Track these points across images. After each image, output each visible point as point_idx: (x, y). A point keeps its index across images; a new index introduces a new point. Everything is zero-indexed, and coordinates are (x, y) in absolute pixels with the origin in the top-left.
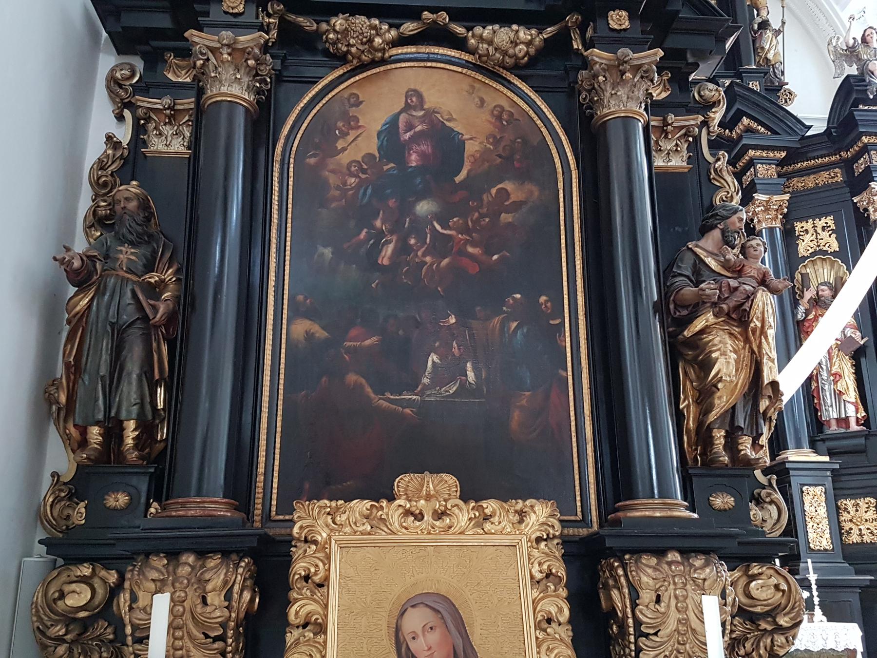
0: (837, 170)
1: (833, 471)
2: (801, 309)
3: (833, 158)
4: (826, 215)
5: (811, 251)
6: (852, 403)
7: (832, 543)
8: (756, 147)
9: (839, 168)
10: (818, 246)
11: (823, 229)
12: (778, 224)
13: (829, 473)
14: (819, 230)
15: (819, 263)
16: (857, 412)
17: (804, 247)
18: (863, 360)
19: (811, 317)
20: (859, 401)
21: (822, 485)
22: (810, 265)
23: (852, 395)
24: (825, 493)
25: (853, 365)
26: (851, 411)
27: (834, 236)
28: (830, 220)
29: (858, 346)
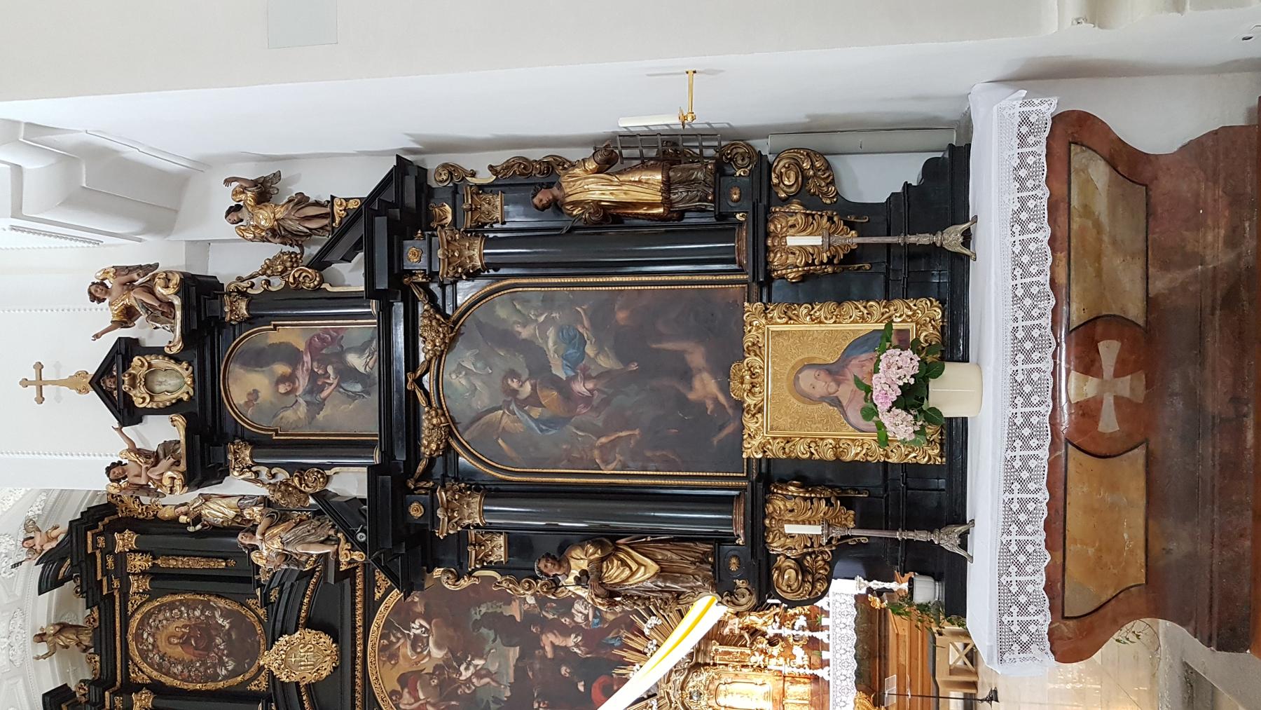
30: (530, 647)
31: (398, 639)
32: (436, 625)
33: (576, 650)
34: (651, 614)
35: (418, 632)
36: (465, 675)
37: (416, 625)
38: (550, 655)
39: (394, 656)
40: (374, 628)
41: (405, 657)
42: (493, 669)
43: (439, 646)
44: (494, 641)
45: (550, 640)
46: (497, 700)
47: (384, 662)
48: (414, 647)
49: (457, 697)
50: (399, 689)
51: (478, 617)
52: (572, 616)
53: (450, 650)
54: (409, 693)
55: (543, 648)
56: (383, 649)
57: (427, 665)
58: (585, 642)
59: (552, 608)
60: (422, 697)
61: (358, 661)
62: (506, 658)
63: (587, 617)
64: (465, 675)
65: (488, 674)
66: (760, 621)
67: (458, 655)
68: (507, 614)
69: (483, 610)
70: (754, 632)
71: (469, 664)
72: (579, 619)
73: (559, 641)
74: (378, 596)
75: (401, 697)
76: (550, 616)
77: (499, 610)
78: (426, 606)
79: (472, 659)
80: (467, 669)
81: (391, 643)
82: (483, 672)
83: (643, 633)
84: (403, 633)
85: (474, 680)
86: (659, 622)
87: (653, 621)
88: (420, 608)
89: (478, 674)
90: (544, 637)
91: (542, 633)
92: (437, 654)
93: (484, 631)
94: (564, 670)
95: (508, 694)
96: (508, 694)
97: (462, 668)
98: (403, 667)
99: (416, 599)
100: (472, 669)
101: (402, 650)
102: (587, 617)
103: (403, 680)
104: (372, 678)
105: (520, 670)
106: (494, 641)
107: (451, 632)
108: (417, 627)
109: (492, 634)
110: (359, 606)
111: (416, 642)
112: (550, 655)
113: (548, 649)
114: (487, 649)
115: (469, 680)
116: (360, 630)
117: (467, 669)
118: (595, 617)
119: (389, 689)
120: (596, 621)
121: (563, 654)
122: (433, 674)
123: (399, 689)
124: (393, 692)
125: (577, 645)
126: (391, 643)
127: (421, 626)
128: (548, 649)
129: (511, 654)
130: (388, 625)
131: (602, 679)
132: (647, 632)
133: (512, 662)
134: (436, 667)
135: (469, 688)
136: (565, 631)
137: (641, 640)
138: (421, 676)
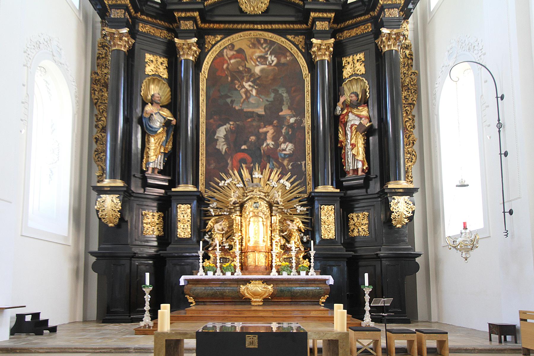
0: (369, 24)
1: (341, 197)
2: (339, 109)
3: (367, 17)
4: (360, 52)
5: (350, 74)
6: (361, 161)
7: (335, 236)
8: (315, 11)
9: (370, 22)
10: (354, 71)
11: (358, 61)
12: (327, 58)
13: (339, 198)
14: (355, 62)
15: (354, 82)
16: (363, 165)
17: (347, 72)
18: (371, 138)
19: (344, 112)
20: (365, 159)
21: (333, 205)
22: (349, 83)
23: (361, 156)
24: (334, 209)
25: (364, 140)
26: (360, 165)
27: (363, 65)
28: (361, 56)
29: (365, 128)
30: (265, 120)
31: (265, 49)
32: (273, 70)
33: (265, 145)
34: (292, 183)
35: (269, 59)
36: (247, 85)
37: (273, 58)
38: (261, 130)
39: (254, 46)
40: (271, 35)
41: (255, 52)
42: (251, 100)
43: (262, 71)
44: (267, 101)
45: (270, 131)
46: (232, 102)
47: (250, 41)
48: (260, 57)
49: (232, 81)
50: (236, 48)
51: (280, 92)
52: (284, 142)
53: (259, 78)
54: (234, 55)
55: (265, 127)
56: (258, 40)
57: (250, 64)
58: (269, 149)
59: (288, 132)
60: (232, 61)
61: (252, 26)
62: (257, 107)
63: (285, 150)
64: (247, 85)
65: (247, 98)
66: (296, 241)
67: (257, 81)
68: (283, 108)
69: (285, 95)
70: (288, 239)
71: (253, 87)
72: (283, 146)
73: (269, 135)
74: (289, 37)
75: (230, 50)
76: (283, 131)
77: (285, 103)
78: (284, 64)
79: (255, 89)
80: (250, 86)
81: (262, 45)
82: (248, 95)
83: (280, 179)
84: (268, 51)
85: (243, 90)
86: (288, 188)
87: (288, 184)
88: (283, 60)
89: (247, 92)
90: (271, 127)
91: (274, 126)
92: (257, 70)
93: (273, 95)
94: (253, 138)
95: (237, 108)
96: (237, 108)
97: (250, 83)
98: (248, 52)
99: (288, 58)
100: (249, 88)
101: (258, 51)
102: (285, 150)
103: (241, 51)
104: (241, 34)
105: (251, 114)
106: (267, 101)
107: (270, 77)
108: (272, 59)
109: (271, 99)
110: (284, 26)
111: (263, 59)
112: (261, 130)
113: (265, 130)
114: (262, 97)
115: (243, 87)
116: (270, 27)
117: (250, 86)
118: (285, 154)
119: (235, 44)
120: (283, 155)
121: (262, 138)
122: (245, 67)
123: (236, 48)
124: (232, 46)
125: (268, 145)
126: (262, 45)
127: (273, 61)
128: (265, 130)
129: (260, 110)
130: (272, 43)
131: (249, 159)
132: (282, 181)
133: (256, 110)
134: (249, 70)
135: (239, 87)
136: (275, 139)
137: (276, 178)
138: (243, 60)
